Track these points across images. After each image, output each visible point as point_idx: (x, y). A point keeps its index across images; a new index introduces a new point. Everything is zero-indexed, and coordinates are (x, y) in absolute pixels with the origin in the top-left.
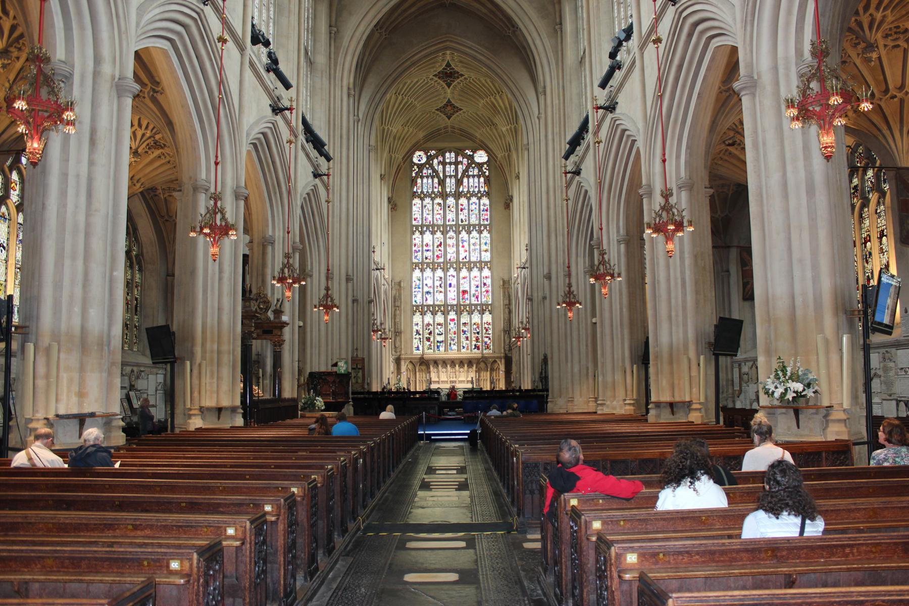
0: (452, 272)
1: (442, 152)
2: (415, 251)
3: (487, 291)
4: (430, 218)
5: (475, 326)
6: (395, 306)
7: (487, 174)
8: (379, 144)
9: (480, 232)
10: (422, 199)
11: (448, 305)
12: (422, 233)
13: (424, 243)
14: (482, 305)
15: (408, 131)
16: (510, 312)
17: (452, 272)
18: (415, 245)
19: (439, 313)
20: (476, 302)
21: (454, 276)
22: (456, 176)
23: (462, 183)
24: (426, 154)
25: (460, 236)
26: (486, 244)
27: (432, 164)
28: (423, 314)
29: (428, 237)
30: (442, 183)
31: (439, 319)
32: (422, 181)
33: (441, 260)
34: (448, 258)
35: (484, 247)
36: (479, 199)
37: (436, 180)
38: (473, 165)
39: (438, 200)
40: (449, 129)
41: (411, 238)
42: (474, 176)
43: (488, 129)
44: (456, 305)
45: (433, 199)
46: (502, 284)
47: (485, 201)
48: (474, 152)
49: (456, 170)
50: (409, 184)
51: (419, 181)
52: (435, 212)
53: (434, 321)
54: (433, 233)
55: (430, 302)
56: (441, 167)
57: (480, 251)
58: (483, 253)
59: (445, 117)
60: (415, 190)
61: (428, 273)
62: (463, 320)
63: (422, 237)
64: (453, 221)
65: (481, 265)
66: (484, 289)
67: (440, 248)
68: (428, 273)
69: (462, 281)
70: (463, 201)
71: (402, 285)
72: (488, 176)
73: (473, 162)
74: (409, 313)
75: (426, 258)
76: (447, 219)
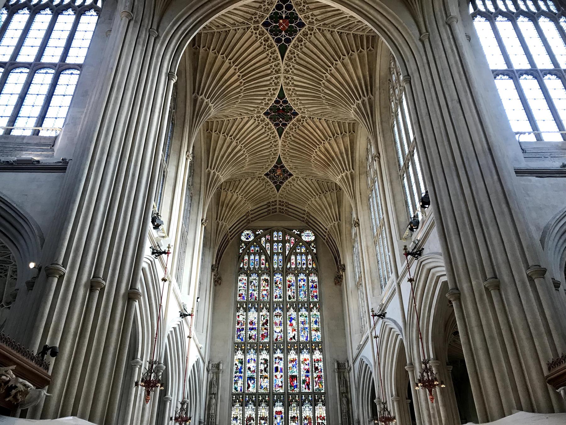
0: (279, 354)
1: (269, 231)
2: (239, 330)
3: (319, 377)
4: (255, 294)
5: (306, 422)
6: (210, 394)
7: (315, 251)
8: (203, 186)
9: (310, 310)
10: (248, 276)
11: (274, 394)
12: (247, 310)
13: (249, 321)
14: (313, 393)
15: (237, 198)
16: (349, 402)
17: (279, 354)
18: (238, 324)
19: (263, 405)
20: (307, 391)
21: (281, 359)
22: (283, 253)
23: (290, 260)
24: (254, 232)
25: (289, 314)
26: (316, 322)
27: (260, 242)
28: (244, 404)
29: (253, 315)
30: (269, 259)
31: (263, 411)
32: (249, 258)
33: (266, 340)
34: (275, 337)
35: (315, 326)
36: (308, 275)
37: (263, 257)
38: (301, 244)
39: (265, 277)
40: (278, 206)
41: (235, 315)
42: (301, 254)
43: (317, 199)
44: (283, 394)
45: (259, 276)
46: (336, 367)
47: (314, 278)
48: (302, 231)
49: (284, 247)
50: (236, 260)
51: (246, 257)
52: (262, 288)
53: (257, 414)
54: (258, 310)
55: (252, 390)
56: (268, 244)
57: (311, 330)
58: (313, 333)
60: (241, 266)
61: (252, 355)
62: (292, 414)
63: (247, 315)
64: (280, 297)
65: (311, 346)
66: (315, 375)
67: (266, 326)
68: (252, 355)
69: (290, 365)
70: (291, 278)
71: (221, 368)
72: (315, 254)
73: (302, 241)
74: (227, 403)
75: (250, 338)
76: (275, 295)
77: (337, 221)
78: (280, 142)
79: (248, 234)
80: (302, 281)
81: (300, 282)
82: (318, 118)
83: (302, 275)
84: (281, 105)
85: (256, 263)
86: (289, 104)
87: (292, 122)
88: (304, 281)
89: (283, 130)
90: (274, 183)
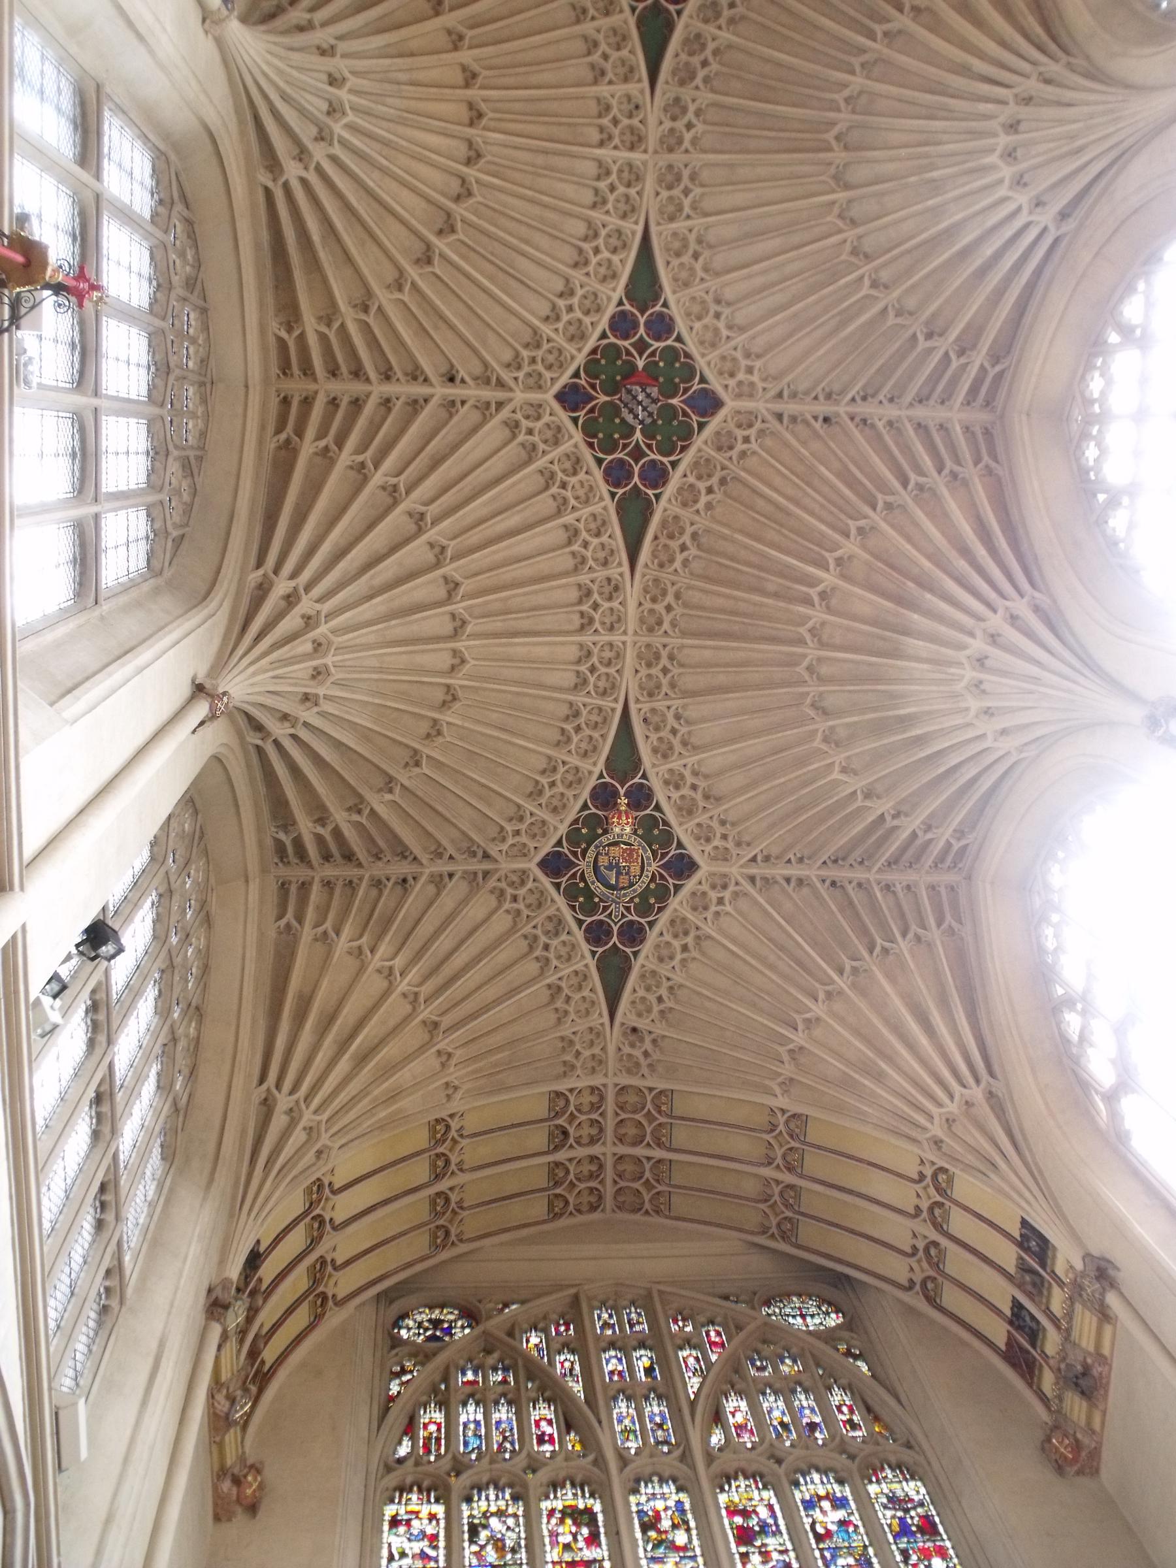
23: (718, 1417)
42: (784, 1391)
59: (586, 958)
60: (404, 1450)
77: (978, 1081)
78: (632, 593)
79: (436, 1323)
80: (826, 1505)
81: (817, 1514)
82: (816, 418)
83: (816, 1477)
84: (641, 346)
85: (496, 1438)
86: (679, 339)
87: (691, 453)
88: (839, 1503)
89: (647, 510)
90: (597, 934)
